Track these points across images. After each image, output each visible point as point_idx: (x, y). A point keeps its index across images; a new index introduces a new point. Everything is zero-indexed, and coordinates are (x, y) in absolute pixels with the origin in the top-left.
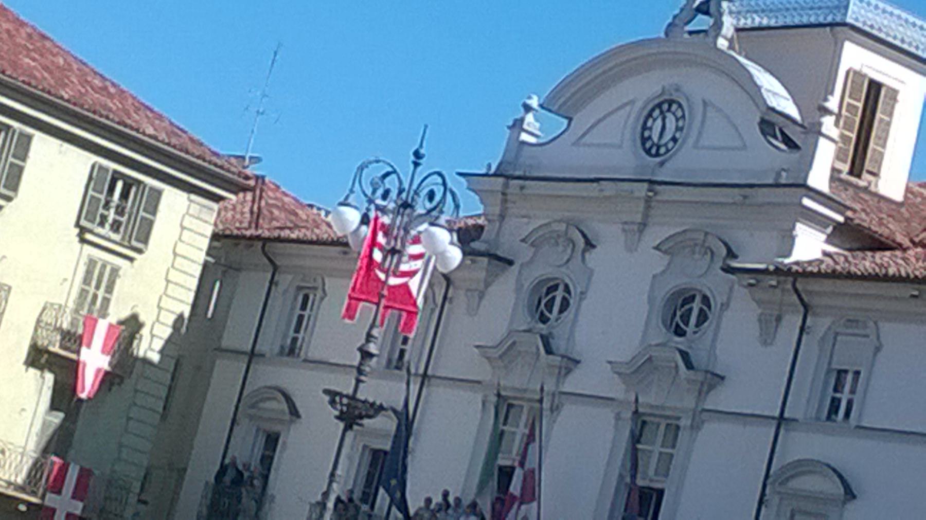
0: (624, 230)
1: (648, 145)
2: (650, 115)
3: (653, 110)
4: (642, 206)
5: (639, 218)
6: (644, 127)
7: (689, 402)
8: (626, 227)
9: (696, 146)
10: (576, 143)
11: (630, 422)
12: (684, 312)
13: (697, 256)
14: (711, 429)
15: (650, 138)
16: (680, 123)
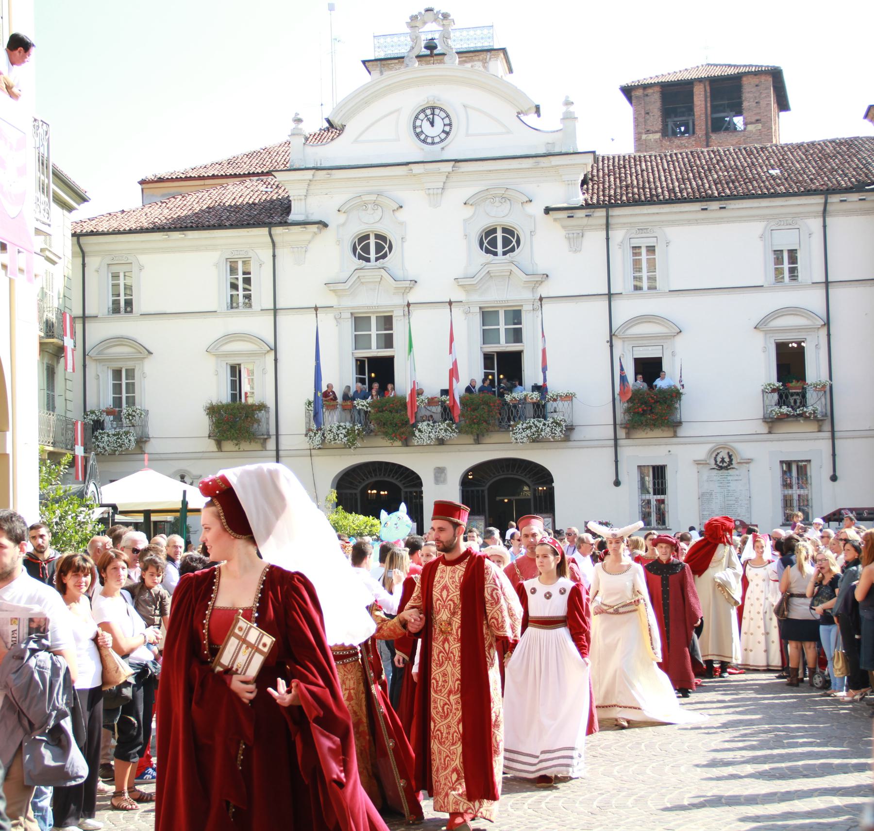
0: (429, 194)
1: (422, 137)
2: (416, 118)
3: (418, 114)
4: (444, 178)
5: (441, 185)
6: (415, 127)
7: (527, 295)
8: (431, 191)
9: (467, 135)
10: (356, 141)
12: (499, 241)
13: (497, 204)
16: (447, 121)
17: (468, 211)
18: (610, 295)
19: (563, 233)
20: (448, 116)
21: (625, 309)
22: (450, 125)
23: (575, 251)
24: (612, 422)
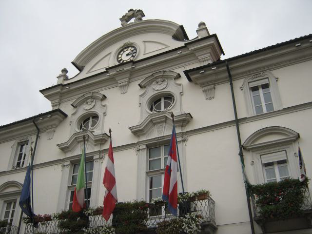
11: (145, 151)
14: (192, 140)
15: (121, 60)
16: (135, 51)
17: (143, 91)
18: (237, 122)
19: (201, 90)
20: (136, 49)
21: (249, 130)
22: (136, 53)
23: (210, 98)
24: (248, 220)
